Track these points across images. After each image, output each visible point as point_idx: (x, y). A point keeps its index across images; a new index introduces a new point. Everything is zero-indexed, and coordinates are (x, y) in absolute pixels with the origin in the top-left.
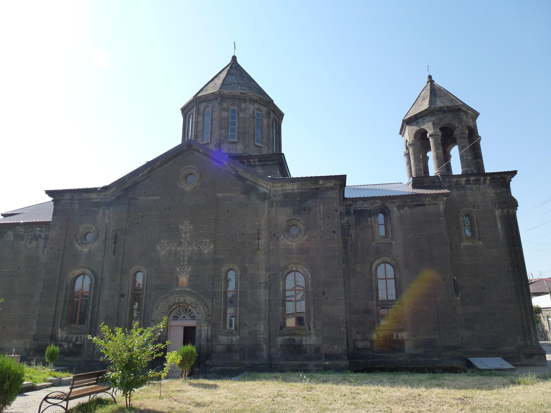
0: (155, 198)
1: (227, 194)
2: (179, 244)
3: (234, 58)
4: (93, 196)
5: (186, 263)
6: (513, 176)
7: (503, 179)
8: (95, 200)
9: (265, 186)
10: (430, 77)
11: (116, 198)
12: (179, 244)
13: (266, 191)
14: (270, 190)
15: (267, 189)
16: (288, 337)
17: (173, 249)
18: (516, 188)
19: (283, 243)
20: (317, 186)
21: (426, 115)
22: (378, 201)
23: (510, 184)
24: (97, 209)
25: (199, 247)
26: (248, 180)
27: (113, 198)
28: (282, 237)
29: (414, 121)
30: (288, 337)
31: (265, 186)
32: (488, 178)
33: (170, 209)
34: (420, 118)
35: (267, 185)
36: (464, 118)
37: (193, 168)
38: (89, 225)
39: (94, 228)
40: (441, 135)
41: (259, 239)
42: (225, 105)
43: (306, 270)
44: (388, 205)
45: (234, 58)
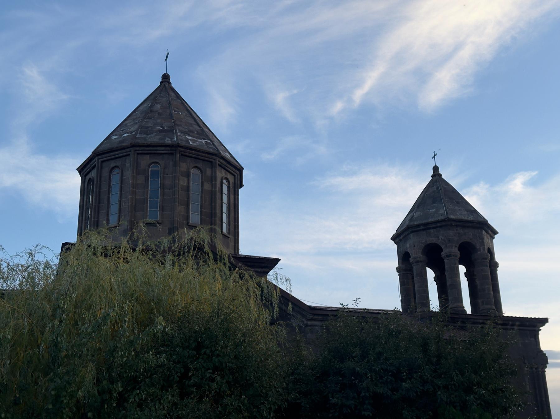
3: (166, 78)
6: (544, 325)
7: (532, 326)
10: (436, 169)
18: (547, 340)
21: (441, 227)
23: (538, 334)
29: (423, 230)
31: (299, 317)
34: (433, 228)
36: (485, 237)
40: (459, 256)
42: (183, 166)
45: (166, 78)
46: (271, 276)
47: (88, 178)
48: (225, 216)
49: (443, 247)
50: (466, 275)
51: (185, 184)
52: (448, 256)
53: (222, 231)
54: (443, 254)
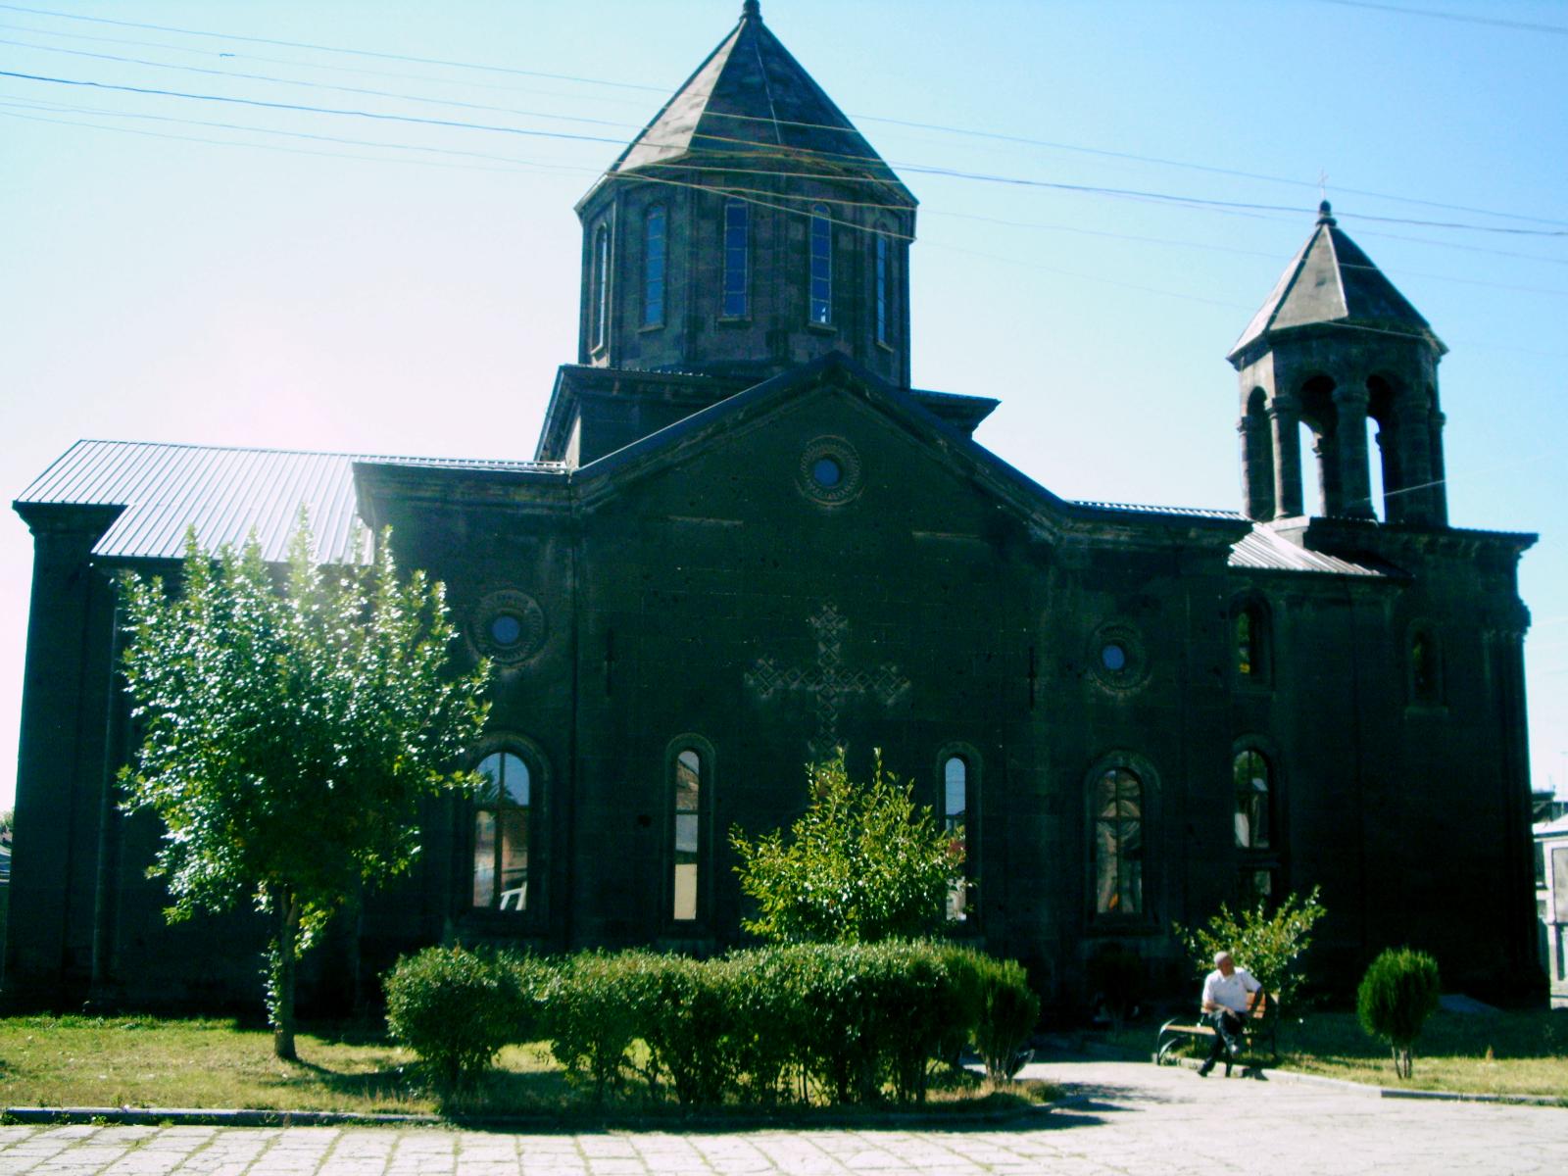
0: (726, 523)
1: (941, 535)
2: (810, 674)
4: (521, 496)
5: (833, 730)
8: (526, 511)
9: (1047, 523)
10: (1325, 207)
11: (598, 511)
12: (810, 674)
13: (1050, 538)
14: (1062, 538)
15: (1052, 534)
16: (1102, 940)
17: (794, 686)
19: (1092, 691)
20: (1179, 541)
22: (1247, 579)
24: (534, 540)
25: (871, 686)
26: (1001, 501)
27: (590, 510)
28: (1090, 676)
30: (1102, 940)
31: (1047, 523)
32: (1477, 544)
33: (776, 565)
35: (1054, 522)
37: (838, 443)
38: (513, 593)
39: (532, 604)
40: (1367, 398)
41: (1032, 675)
43: (1152, 769)
44: (1268, 591)
46: (985, 435)
47: (596, 227)
48: (881, 305)
49: (1336, 378)
50: (1379, 438)
51: (800, 237)
52: (1347, 398)
53: (875, 340)
54: (1336, 394)
